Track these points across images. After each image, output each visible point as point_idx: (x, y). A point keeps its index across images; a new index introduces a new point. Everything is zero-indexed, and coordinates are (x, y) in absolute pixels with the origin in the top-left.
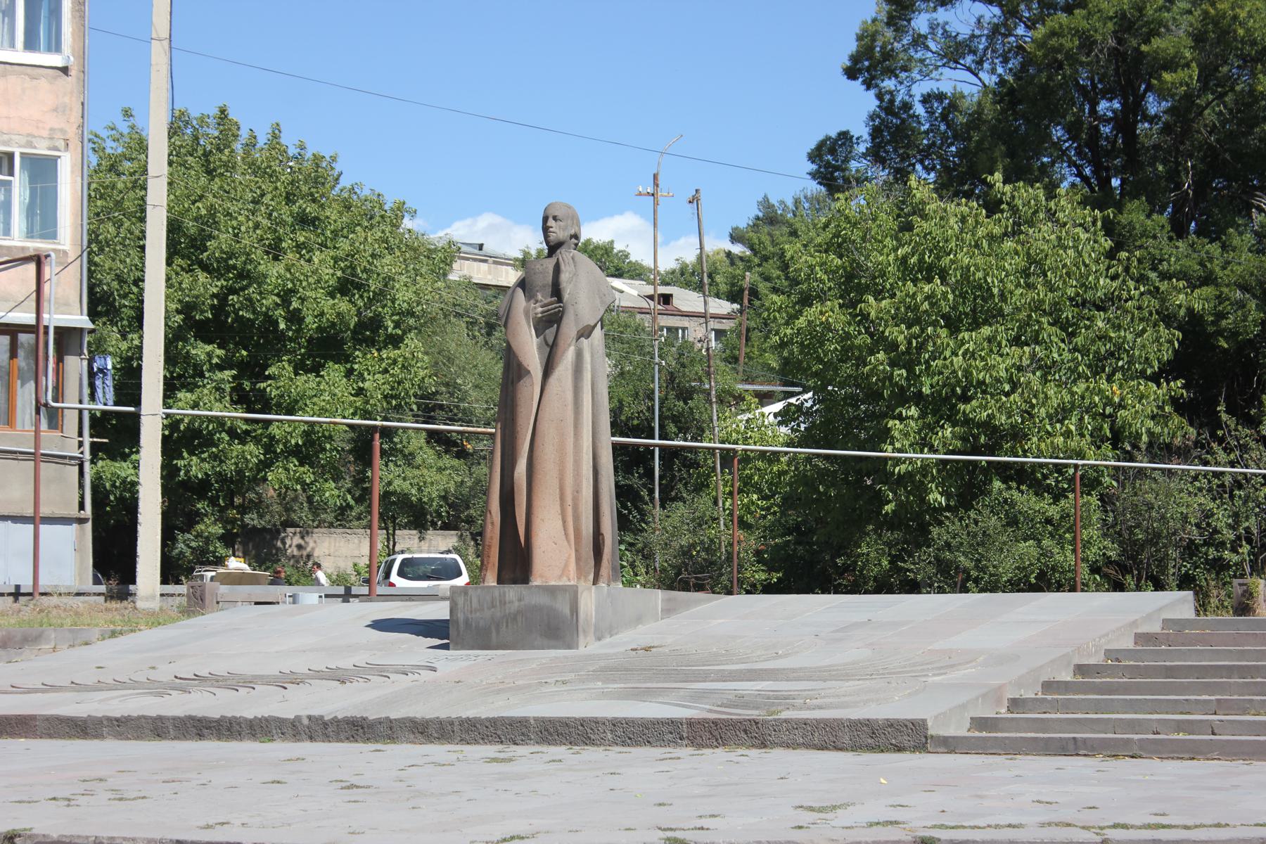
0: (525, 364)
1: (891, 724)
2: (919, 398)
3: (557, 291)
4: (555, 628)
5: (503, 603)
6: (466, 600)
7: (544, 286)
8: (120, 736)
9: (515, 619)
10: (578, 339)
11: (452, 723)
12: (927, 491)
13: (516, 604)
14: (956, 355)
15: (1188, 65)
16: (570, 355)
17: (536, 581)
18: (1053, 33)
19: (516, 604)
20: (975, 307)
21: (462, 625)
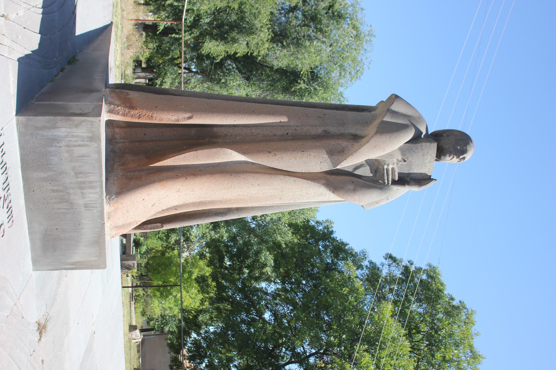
5: (82, 186)
13: (81, 202)
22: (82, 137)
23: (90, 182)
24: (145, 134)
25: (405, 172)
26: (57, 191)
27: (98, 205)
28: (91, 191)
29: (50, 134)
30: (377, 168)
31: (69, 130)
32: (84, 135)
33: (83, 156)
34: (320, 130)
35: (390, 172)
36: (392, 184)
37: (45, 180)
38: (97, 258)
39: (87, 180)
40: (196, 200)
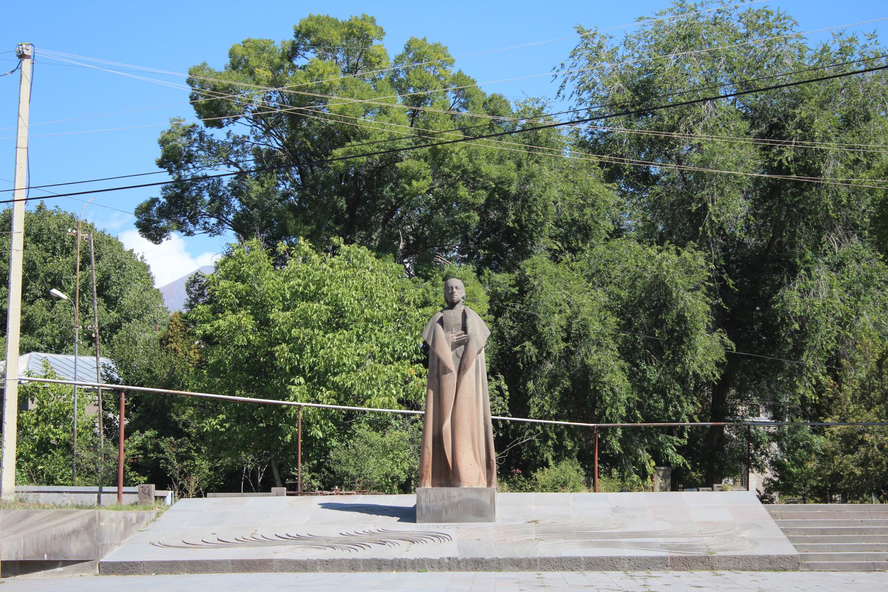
1: (780, 557)
3: (464, 328)
4: (481, 512)
5: (450, 497)
8: (327, 570)
11: (536, 561)
13: (458, 498)
16: (474, 362)
20: (337, 320)
21: (424, 510)
34: (436, 380)
40: (470, 443)
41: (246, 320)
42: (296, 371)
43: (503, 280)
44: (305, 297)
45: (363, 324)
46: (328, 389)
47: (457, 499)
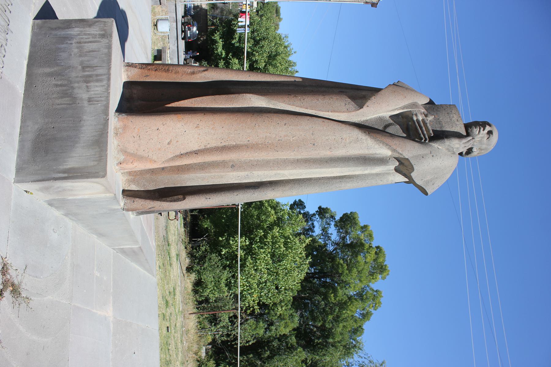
0: (369, 103)
2: (251, 244)
3: (440, 135)
5: (87, 80)
6: (94, 36)
7: (440, 123)
9: (65, 94)
10: (397, 159)
12: (226, 248)
13: (85, 96)
14: (264, 255)
15: (335, 299)
16: (384, 151)
17: (115, 121)
18: (342, 265)
19: (85, 96)
20: (277, 258)
21: (62, 33)
22: (93, 34)
23: (97, 75)
24: (162, 94)
25: (438, 129)
26: (61, 85)
27: (103, 99)
28: (97, 84)
29: (63, 33)
30: (408, 125)
31: (82, 29)
32: (96, 32)
33: (93, 51)
35: (422, 125)
36: (429, 141)
37: (50, 75)
38: (96, 163)
39: (95, 73)
40: (219, 144)
41: (273, 218)
42: (252, 241)
43: (293, 340)
44: (286, 244)
45: (275, 271)
46: (245, 255)
47: (82, 94)
